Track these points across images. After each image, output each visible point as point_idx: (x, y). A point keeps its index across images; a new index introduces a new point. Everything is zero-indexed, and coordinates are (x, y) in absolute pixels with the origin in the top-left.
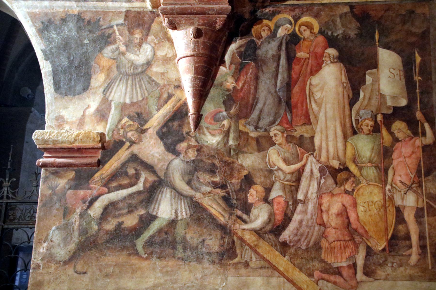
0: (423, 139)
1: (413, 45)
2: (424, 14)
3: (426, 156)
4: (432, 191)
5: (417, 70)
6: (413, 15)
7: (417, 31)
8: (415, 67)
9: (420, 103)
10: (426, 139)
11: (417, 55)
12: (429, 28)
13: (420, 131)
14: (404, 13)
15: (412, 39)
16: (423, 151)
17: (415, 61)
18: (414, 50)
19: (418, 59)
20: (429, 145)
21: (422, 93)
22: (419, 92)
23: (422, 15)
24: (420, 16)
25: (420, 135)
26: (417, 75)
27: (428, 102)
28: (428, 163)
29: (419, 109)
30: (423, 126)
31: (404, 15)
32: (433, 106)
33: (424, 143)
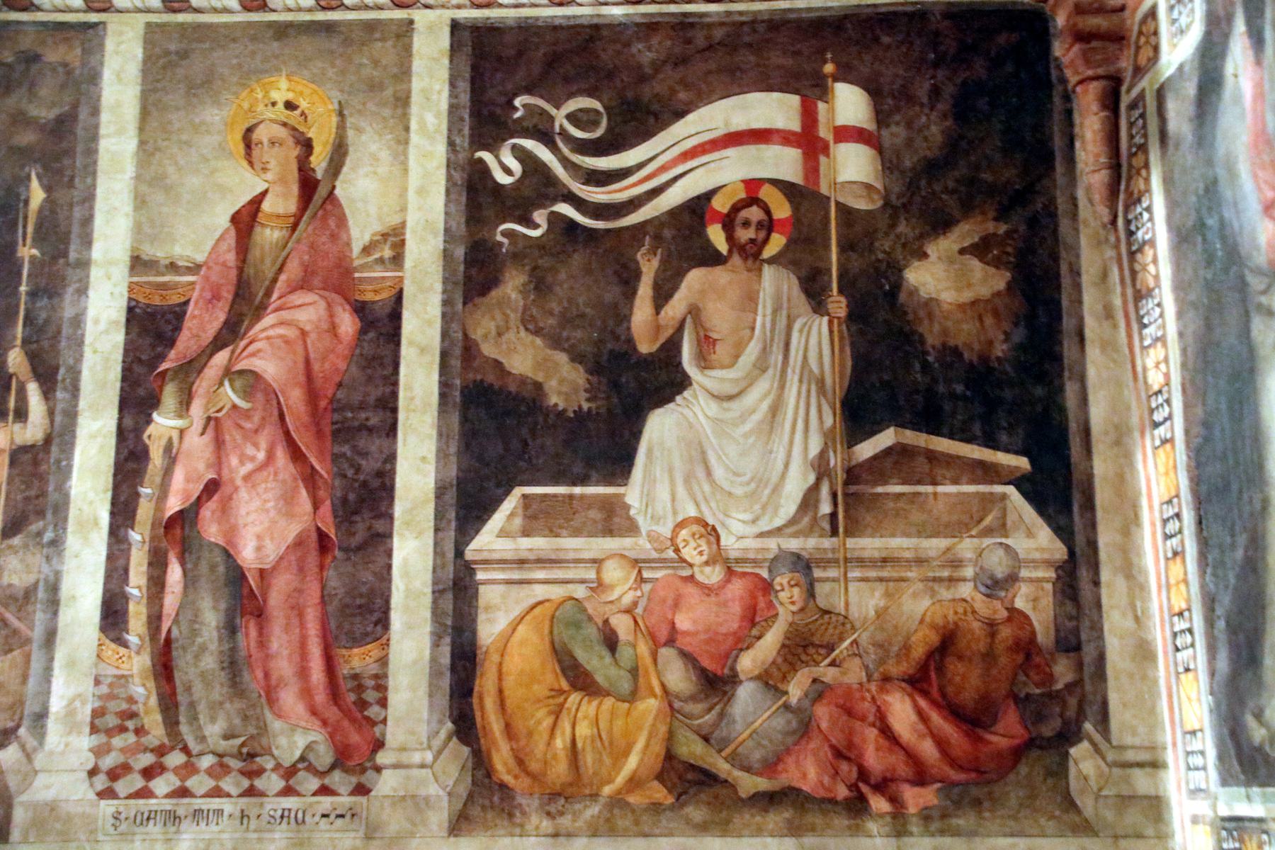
0: (17, 427)
1: (24, 155)
2: (65, 65)
3: (17, 480)
4: (15, 581)
5: (30, 229)
6: (35, 68)
7: (43, 114)
8: (26, 218)
9: (25, 325)
10: (25, 428)
11: (35, 183)
12: (75, 106)
13: (12, 404)
14: (10, 60)
15: (27, 138)
16: (13, 462)
17: (27, 202)
18: (27, 169)
19: (37, 195)
20: (33, 446)
21: (33, 295)
22: (28, 293)
23: (60, 69)
24: (54, 70)
25: (11, 418)
26: (29, 241)
27: (47, 321)
28: (19, 497)
29: (19, 342)
30: (22, 392)
31: (9, 66)
32: (59, 332)
33: (19, 441)
